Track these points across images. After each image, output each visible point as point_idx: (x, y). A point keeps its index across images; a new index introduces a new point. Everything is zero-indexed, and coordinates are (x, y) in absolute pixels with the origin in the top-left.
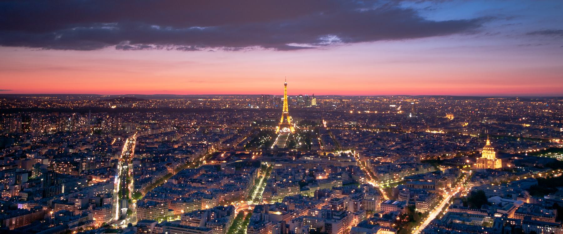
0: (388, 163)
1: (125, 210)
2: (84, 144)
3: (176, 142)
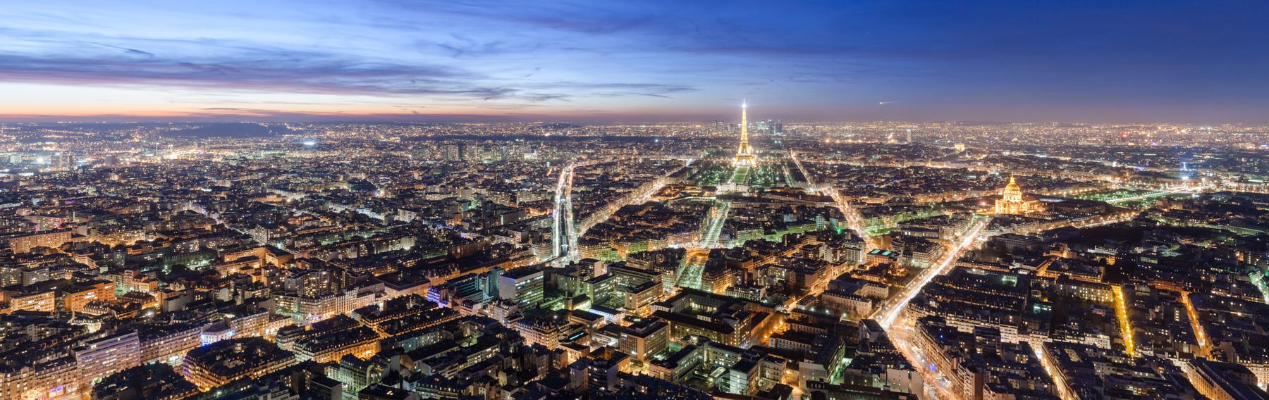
3: (617, 175)
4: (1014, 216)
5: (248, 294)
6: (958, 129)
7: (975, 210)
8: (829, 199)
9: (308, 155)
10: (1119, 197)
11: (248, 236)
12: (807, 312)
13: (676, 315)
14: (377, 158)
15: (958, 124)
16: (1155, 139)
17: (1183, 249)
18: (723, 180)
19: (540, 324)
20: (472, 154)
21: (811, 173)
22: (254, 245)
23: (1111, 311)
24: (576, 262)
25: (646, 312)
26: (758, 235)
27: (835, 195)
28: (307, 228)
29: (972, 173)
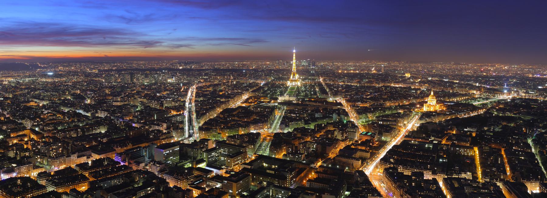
3: (221, 91)
4: (432, 112)
5: (23, 154)
6: (407, 65)
7: (414, 110)
8: (340, 104)
9: (50, 80)
10: (479, 101)
11: (21, 124)
12: (327, 167)
13: (255, 169)
14: (86, 82)
15: (407, 63)
16: (494, 71)
17: (504, 127)
18: (282, 94)
19: (177, 175)
20: (138, 79)
21: (331, 90)
22: (24, 128)
23: (473, 158)
24: (198, 140)
25: (237, 168)
26: (301, 125)
27: (343, 102)
28: (50, 120)
29: (414, 89)
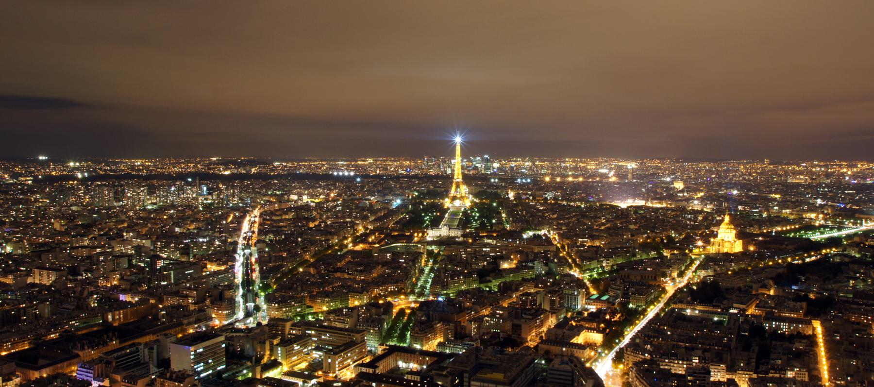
0: (597, 247)
1: (251, 305)
2: (192, 222)
18: (435, 224)
24: (265, 322)
